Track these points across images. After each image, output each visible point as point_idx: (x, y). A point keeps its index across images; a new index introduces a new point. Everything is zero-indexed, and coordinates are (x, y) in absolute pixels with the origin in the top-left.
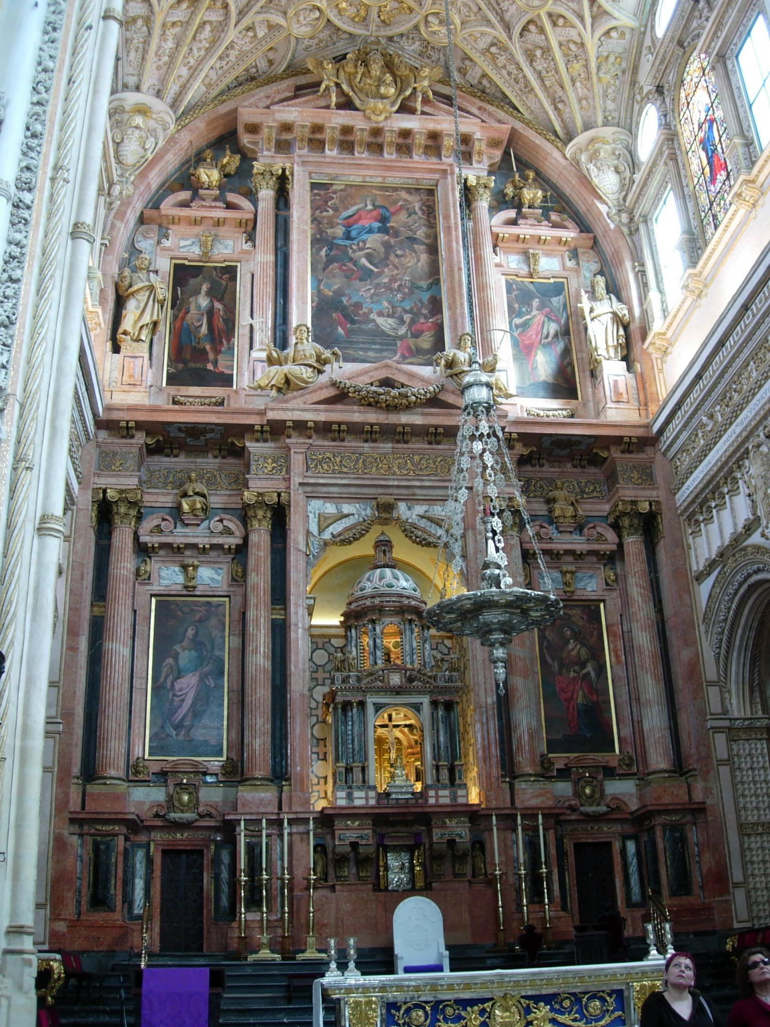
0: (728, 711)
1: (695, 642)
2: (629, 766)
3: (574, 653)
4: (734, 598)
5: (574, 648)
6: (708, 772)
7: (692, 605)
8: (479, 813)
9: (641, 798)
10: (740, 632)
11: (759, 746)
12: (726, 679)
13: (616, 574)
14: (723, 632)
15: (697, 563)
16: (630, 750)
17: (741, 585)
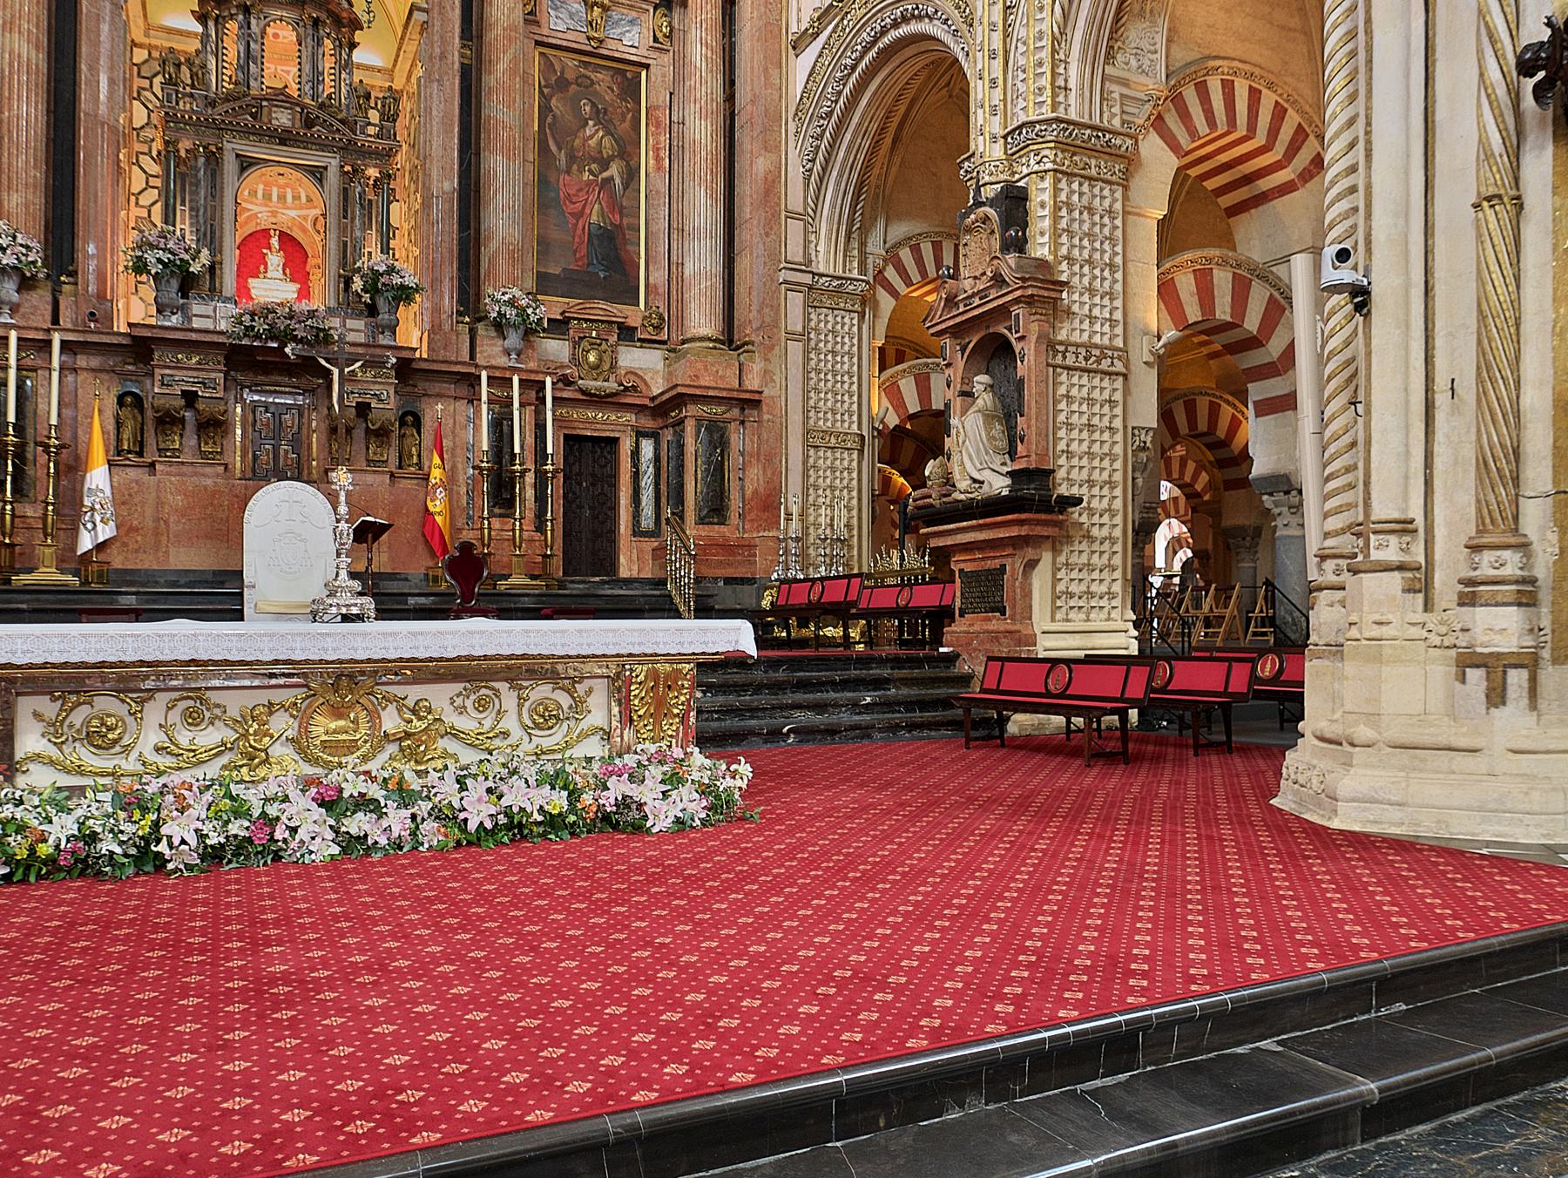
0: (811, 261)
1: (778, 148)
2: (658, 328)
3: (592, 142)
4: (849, 75)
5: (593, 135)
6: (772, 348)
7: (781, 89)
8: (414, 365)
9: (670, 375)
10: (848, 136)
11: (847, 320)
12: (815, 212)
13: (670, 24)
14: (822, 136)
15: (799, 21)
16: (661, 305)
17: (866, 50)
